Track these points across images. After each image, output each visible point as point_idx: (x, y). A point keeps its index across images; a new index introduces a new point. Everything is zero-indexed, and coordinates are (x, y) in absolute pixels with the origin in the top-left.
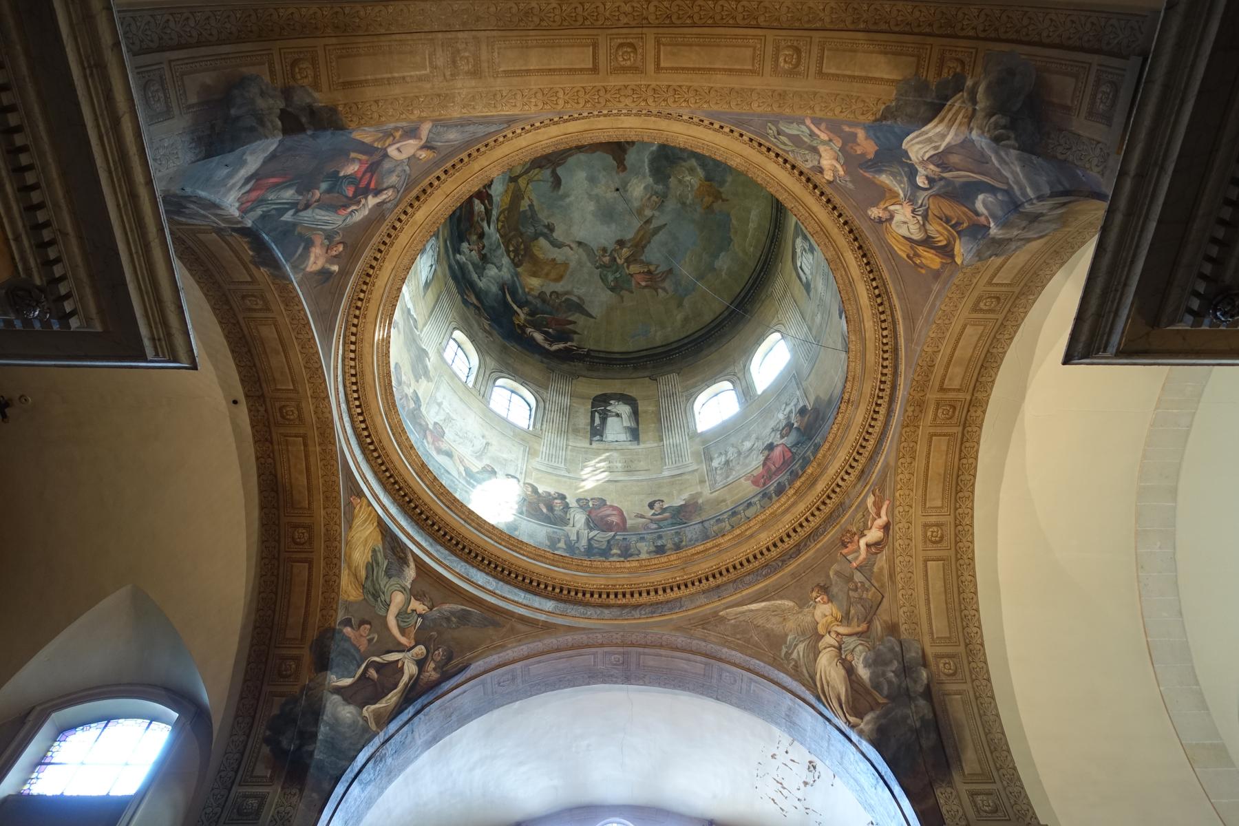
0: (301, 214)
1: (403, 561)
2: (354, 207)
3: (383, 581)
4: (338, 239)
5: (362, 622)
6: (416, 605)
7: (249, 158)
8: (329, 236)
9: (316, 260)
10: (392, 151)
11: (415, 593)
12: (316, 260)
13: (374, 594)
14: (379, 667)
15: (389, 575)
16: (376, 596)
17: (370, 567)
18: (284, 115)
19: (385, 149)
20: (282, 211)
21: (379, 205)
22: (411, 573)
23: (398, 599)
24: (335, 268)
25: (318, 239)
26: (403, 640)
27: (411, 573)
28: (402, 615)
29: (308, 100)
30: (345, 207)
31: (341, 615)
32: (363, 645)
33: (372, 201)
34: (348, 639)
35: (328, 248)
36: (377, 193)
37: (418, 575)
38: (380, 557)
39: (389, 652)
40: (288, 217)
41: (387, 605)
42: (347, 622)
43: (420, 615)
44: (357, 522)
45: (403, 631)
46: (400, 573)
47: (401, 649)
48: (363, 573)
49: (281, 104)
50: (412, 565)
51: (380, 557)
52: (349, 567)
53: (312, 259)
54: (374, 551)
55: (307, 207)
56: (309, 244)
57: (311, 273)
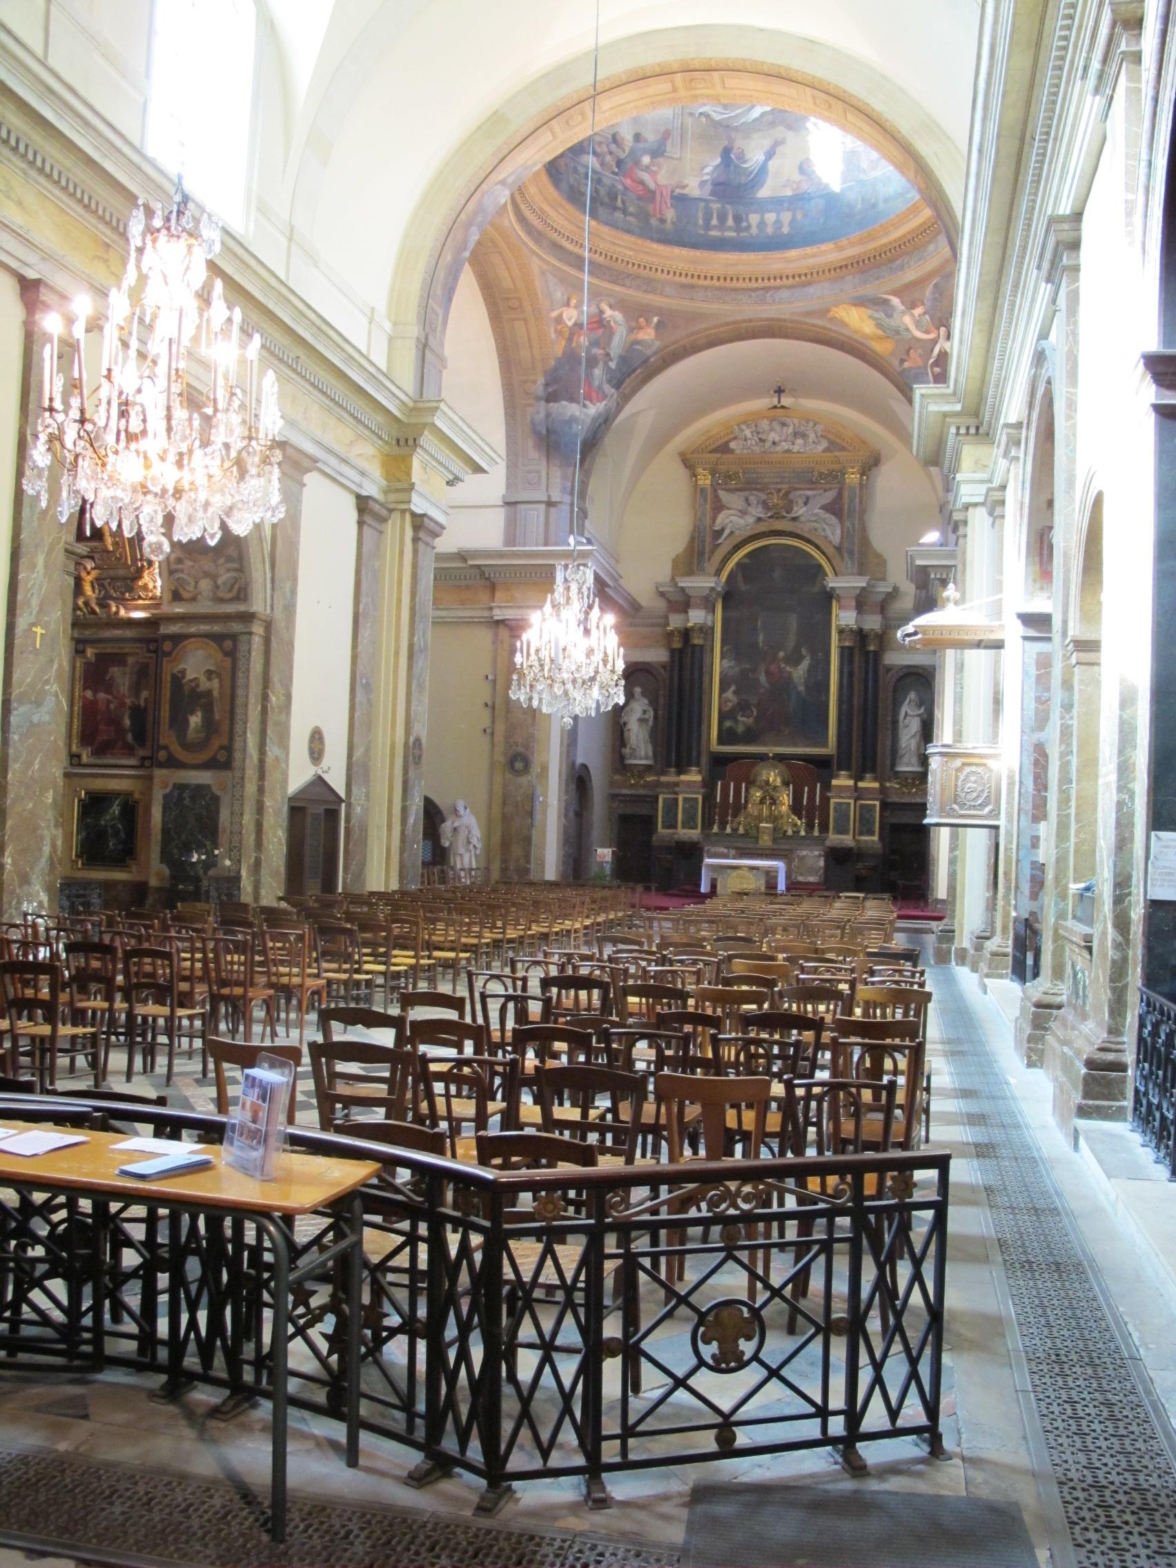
0: (612, 355)
1: (886, 302)
2: (612, 324)
3: (892, 322)
4: (634, 324)
5: (908, 352)
6: (918, 311)
7: (569, 414)
8: (631, 330)
9: (648, 334)
10: (570, 324)
11: (912, 306)
12: (648, 334)
13: (896, 333)
14: (936, 364)
15: (889, 316)
16: (898, 333)
17: (879, 325)
18: (548, 400)
19: (570, 328)
20: (609, 369)
21: (611, 306)
22: (895, 301)
23: (907, 320)
24: (655, 319)
25: (633, 337)
26: (932, 336)
27: (895, 301)
28: (918, 324)
29: (541, 388)
30: (611, 328)
31: (896, 363)
32: (920, 363)
33: (608, 313)
34: (910, 369)
35: (640, 328)
36: (602, 312)
37: (900, 297)
38: (876, 315)
39: (932, 350)
40: (613, 365)
41: (908, 330)
42: (902, 361)
43: (925, 313)
44: (846, 319)
45: (927, 332)
46: (893, 308)
47: (935, 342)
48: (880, 332)
49: (543, 403)
50: (891, 297)
51: (876, 315)
52: (872, 339)
53: (646, 337)
54: (870, 317)
55: (608, 355)
56: (637, 342)
57: (657, 336)
